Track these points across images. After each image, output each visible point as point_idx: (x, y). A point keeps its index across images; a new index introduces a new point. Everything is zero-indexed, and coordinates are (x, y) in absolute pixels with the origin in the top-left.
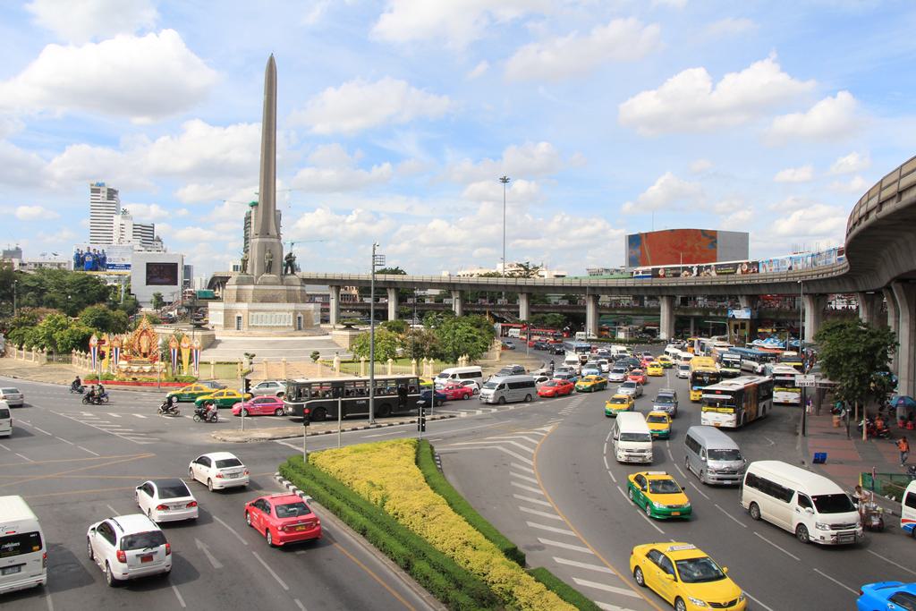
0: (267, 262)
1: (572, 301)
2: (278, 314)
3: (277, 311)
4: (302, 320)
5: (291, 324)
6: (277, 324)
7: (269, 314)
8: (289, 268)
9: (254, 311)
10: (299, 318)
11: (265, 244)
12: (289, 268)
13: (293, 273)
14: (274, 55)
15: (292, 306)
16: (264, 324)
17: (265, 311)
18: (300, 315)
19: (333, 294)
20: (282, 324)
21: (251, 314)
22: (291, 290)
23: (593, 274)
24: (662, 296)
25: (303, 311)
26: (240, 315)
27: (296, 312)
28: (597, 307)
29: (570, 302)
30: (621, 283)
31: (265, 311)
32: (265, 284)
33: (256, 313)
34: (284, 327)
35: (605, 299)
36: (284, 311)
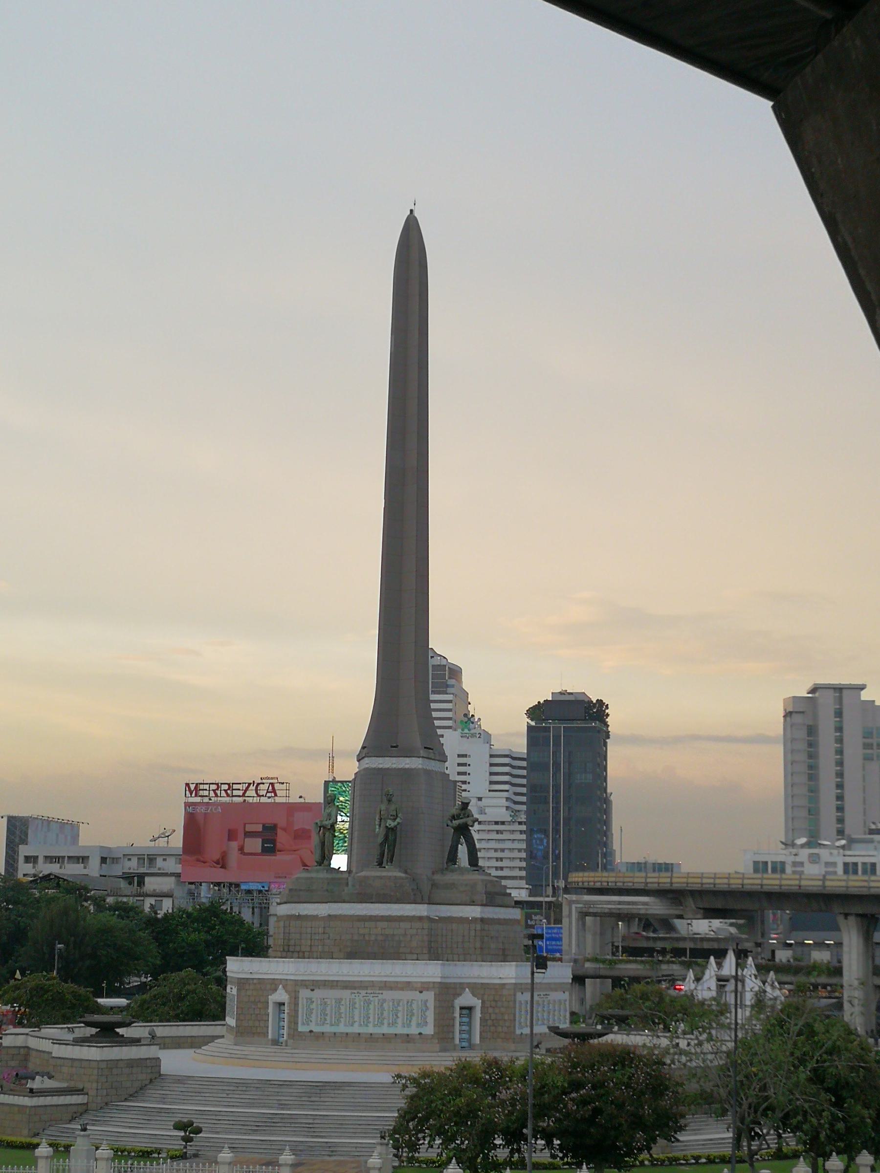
0: (380, 831)
2: (388, 995)
3: (386, 986)
4: (478, 1014)
5: (429, 1030)
6: (385, 1030)
8: (463, 850)
9: (314, 985)
10: (470, 1009)
12: (463, 850)
13: (473, 860)
14: (416, 214)
15: (431, 971)
16: (342, 1029)
18: (467, 999)
20: (400, 1030)
21: (304, 993)
22: (442, 919)
24: (846, 915)
25: (478, 989)
26: (281, 995)
27: (446, 992)
33: (318, 994)
34: (408, 1038)
36: (408, 986)
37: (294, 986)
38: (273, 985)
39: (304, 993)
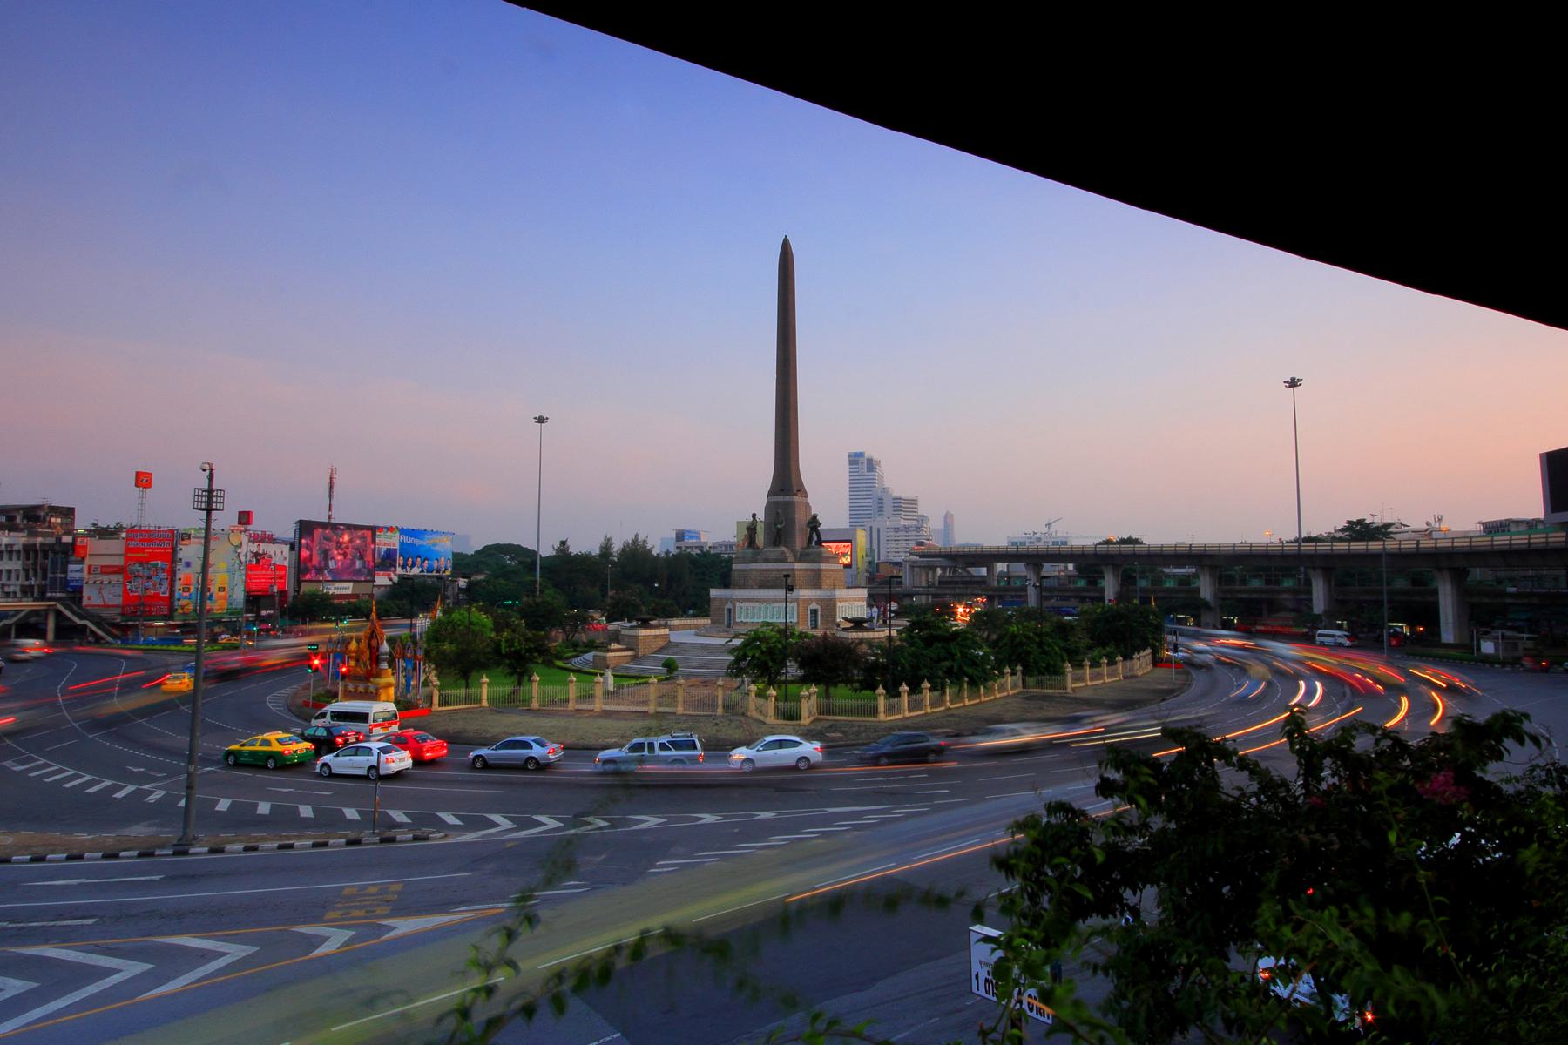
1: (1418, 581)
7: (763, 606)
10: (814, 611)
11: (777, 503)
17: (758, 601)
18: (814, 606)
19: (1031, 575)
23: (1492, 528)
25: (818, 601)
26: (729, 606)
28: (1464, 593)
29: (1415, 582)
30: (1538, 538)
31: (758, 601)
32: (767, 561)
35: (1477, 574)
37: (733, 601)
38: (727, 601)
39: (738, 605)
